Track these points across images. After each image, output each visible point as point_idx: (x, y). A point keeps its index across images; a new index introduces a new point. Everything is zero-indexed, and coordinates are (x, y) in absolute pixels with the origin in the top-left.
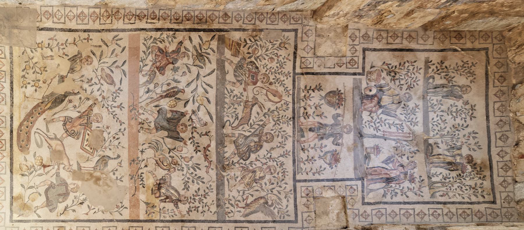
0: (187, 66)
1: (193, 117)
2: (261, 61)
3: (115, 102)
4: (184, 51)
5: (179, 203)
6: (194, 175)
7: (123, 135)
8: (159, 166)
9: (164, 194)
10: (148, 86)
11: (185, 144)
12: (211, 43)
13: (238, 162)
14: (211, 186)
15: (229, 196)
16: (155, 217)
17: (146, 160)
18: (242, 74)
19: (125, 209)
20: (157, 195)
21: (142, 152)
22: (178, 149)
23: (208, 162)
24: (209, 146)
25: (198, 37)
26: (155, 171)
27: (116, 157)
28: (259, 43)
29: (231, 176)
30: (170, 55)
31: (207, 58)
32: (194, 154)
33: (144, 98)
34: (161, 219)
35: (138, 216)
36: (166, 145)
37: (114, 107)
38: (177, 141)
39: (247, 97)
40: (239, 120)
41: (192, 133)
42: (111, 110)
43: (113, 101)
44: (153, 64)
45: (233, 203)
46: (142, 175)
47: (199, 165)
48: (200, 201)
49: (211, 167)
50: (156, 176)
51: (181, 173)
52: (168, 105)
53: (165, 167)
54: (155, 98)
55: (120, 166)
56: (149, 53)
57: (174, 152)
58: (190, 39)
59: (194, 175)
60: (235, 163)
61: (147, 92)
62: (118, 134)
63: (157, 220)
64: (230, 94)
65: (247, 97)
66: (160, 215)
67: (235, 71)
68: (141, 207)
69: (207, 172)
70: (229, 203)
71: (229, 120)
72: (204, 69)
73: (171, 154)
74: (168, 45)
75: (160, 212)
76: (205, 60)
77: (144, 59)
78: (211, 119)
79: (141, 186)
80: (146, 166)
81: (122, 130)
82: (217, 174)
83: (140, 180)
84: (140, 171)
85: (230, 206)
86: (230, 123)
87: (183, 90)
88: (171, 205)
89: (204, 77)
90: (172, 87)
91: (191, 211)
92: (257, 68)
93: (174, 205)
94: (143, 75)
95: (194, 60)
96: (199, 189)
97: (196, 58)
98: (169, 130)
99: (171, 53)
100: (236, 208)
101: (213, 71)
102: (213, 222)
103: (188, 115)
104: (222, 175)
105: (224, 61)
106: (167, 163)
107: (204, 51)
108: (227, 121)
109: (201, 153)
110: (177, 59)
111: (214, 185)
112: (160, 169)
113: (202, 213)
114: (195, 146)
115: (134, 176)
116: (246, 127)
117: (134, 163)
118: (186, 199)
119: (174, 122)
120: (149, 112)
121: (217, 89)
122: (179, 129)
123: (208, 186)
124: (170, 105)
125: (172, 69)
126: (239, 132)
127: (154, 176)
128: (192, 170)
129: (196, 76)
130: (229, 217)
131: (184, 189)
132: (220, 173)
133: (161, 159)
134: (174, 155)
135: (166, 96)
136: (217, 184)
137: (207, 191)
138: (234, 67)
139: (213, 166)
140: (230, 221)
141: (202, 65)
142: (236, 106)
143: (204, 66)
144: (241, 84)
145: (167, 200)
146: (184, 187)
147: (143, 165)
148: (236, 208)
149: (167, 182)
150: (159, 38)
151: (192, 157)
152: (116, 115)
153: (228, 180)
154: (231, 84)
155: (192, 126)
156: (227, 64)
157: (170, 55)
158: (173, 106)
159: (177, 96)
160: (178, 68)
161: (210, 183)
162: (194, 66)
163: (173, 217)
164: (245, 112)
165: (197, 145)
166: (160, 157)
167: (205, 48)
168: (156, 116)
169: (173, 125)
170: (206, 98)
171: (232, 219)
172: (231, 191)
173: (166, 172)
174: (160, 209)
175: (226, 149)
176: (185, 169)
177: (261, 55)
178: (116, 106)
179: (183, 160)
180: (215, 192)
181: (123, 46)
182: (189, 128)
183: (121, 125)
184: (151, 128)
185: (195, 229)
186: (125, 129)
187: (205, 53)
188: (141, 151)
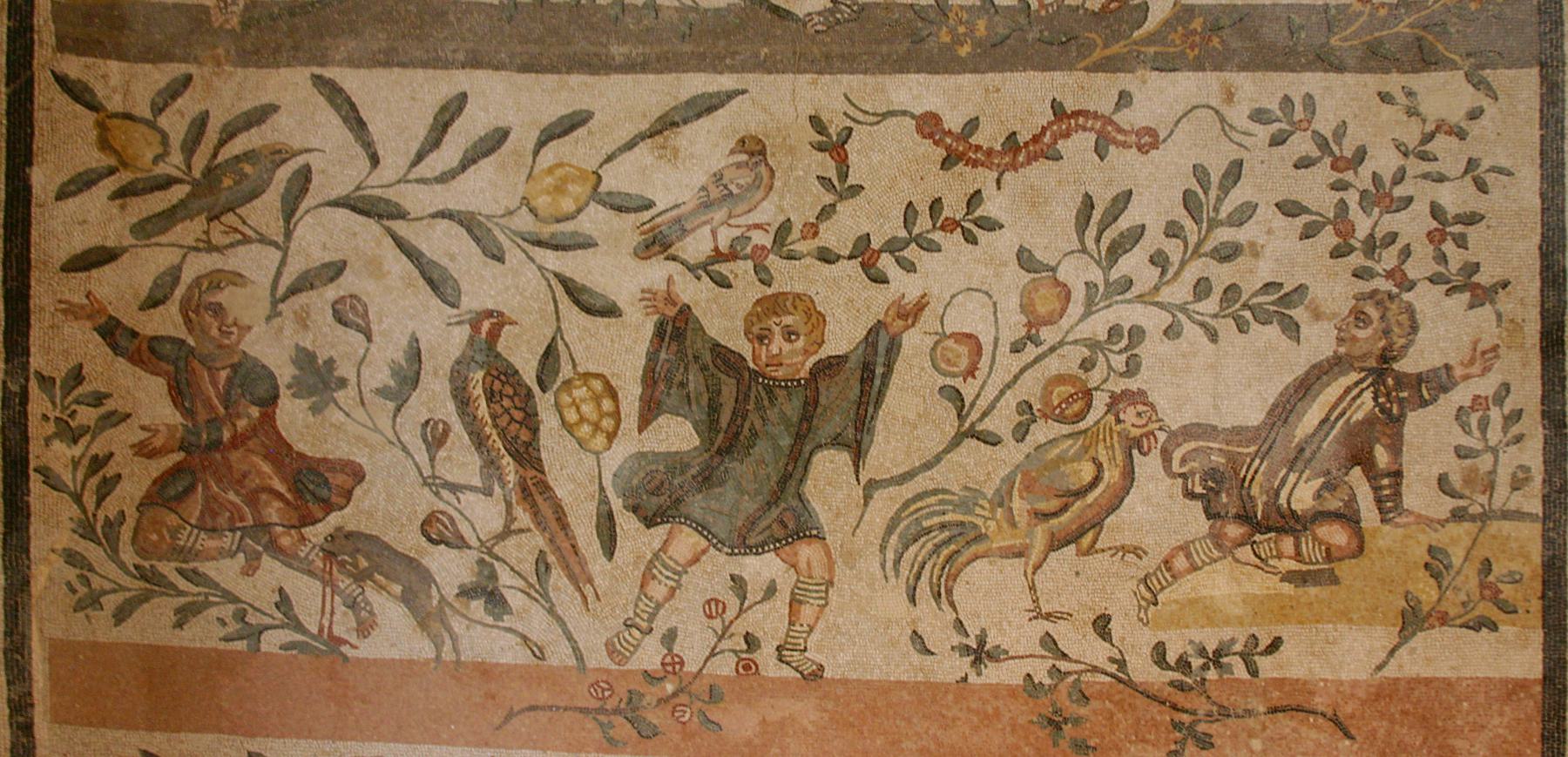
5: (1405, 366)
16: (1527, 557)
22: (964, 363)
34: (1536, 507)
36: (928, 466)
38: (895, 379)
41: (826, 257)
51: (1153, 349)
53: (1111, 475)
57: (982, 403)
63: (1547, 542)
66: (1506, 515)
73: (1001, 422)
88: (1416, 423)
98: (799, 438)
106: (1077, 458)
112: (1122, 512)
119: (742, 398)
133: (1043, 506)
134: (1011, 400)
145: (1382, 457)
149: (1233, 459)
155: (772, 261)
166: (1022, 519)
173: (1148, 466)
182: (788, 277)
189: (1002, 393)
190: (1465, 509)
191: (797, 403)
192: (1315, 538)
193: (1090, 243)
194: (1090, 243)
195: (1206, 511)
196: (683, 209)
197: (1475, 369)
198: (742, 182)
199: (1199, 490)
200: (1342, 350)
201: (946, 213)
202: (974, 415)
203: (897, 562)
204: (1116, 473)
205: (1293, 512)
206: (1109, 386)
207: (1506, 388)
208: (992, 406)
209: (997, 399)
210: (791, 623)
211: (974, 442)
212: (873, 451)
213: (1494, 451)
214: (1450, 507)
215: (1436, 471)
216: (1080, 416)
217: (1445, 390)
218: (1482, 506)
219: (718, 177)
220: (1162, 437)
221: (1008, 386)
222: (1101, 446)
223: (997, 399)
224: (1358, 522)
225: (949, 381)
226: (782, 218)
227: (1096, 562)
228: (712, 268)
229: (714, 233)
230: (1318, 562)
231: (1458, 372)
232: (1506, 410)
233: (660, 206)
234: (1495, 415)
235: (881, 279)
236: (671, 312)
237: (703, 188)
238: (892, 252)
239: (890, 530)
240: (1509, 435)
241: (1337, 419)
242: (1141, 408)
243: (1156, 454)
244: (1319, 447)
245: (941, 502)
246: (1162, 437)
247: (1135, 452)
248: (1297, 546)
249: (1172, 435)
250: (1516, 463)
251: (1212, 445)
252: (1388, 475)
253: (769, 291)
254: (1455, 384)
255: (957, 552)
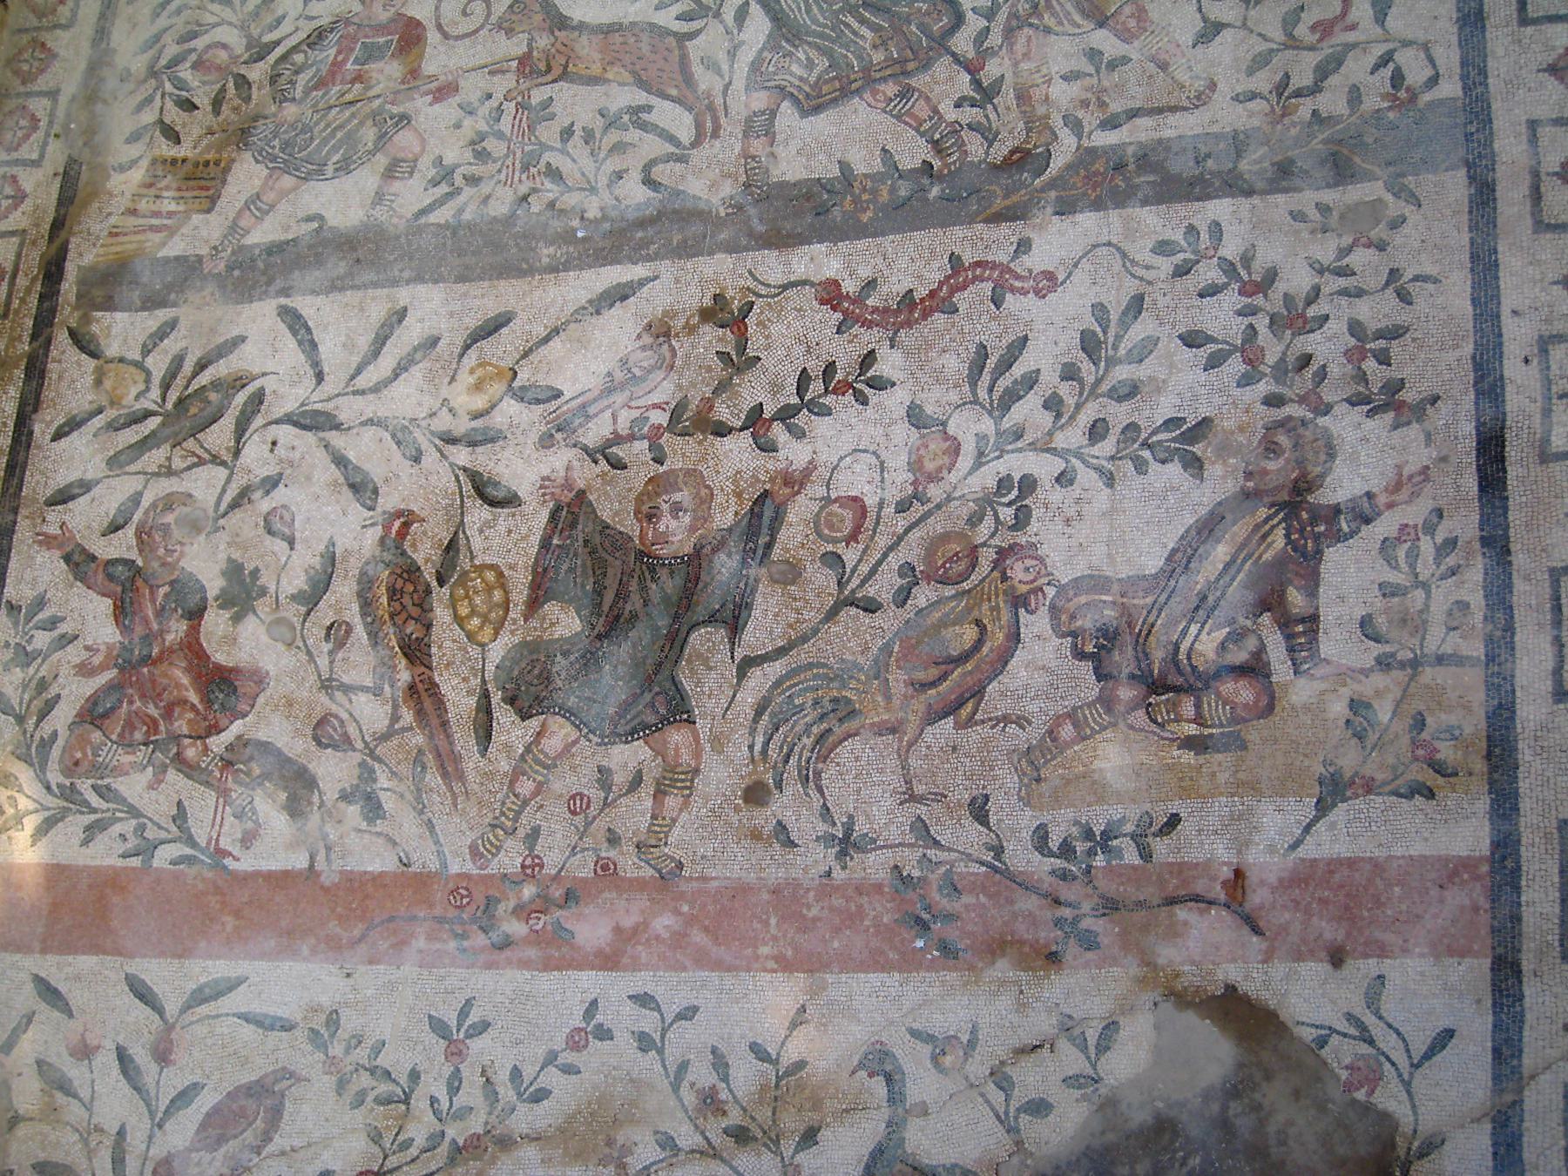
0: (235, 505)
1: (596, 432)
2: (279, 21)
3: (415, 1076)
4: (130, 532)
6: (1066, 391)
7: (688, 1014)
8: (978, 693)
9: (1237, 636)
10: (331, 795)
11: (795, 481)
12: (112, 349)
13: (972, 69)
14: (1164, 248)
15: (1253, 96)
16: (1467, 708)
17: (922, 810)
18: (340, 127)
19: (1389, 1007)
20: (1244, 692)
21: (847, 844)
23: (964, 288)
24: (831, 295)
25: (64, 442)
26: (1022, 721)
27: (879, 1087)
28: (172, 50)
29: (1085, 104)
30: (139, 630)
31: (201, 366)
32: (895, 401)
33: (408, 826)
34: (1477, 649)
35: (1455, 871)
36: (804, 639)
37: (454, 1089)
39: (496, 70)
40: (654, 101)
41: (722, 430)
42: (476, 1125)
43: (406, 1101)
44: (180, 761)
45: (1310, 60)
46: (1054, 843)
47: (982, 352)
48: (1294, 320)
49: (1002, 257)
50: (1071, 715)
52: (488, 631)
53: (998, 637)
54: (418, 739)
55: (972, 1044)
56: (103, 792)
57: (864, 569)
58: (63, 497)
59: (1066, 391)
60: (977, 83)
61: (373, 809)
62: (683, 1067)
63: (1491, 687)
64: (458, 180)
65: (496, 70)
66: (1440, 660)
67: (318, 172)
68: (1366, 848)
69: (1048, 282)
70: (1315, 89)
71: (647, 168)
72: (269, 384)
74: (74, 654)
75: (1415, 664)
76: (216, 385)
77: (141, 828)
78: (624, 298)
79: (1161, 848)
80: (979, 808)
81: (648, 1022)
82: (1065, 209)
83: (1099, 861)
84: (1022, 857)
85: (1333, 80)
86: (669, 158)
87: (387, 528)
88: (1336, 560)
89: (320, 377)
90: (355, 607)
91: (1401, 384)
92: (316, 38)
93: (1340, 537)
94: (247, 840)
95: (201, 462)
96: (1192, 340)
97: (190, 444)
99: (125, 629)
100: (1351, 37)
101: (295, 321)
102: (1484, 195)
103: (575, 474)
104: (1069, 167)
105: (242, 248)
107: (155, 393)
108: (649, 182)
109: (883, 351)
110: (172, 583)
111: (1154, 222)
113: (1404, 297)
114: (829, 400)
115: (1067, 912)
116: (709, 41)
117: (950, 917)
118: (1283, 439)
120: (525, 787)
121: (419, 279)
122: (676, 533)
123: (1166, 265)
124: (485, 619)
125: (237, 619)
126: (739, 84)
127: (1067, 731)
128: (1028, 410)
129: (310, 437)
130: (1434, 81)
131: (1194, 465)
132: (1052, 184)
133: (920, 675)
135: (416, 652)
136: (1145, 202)
137: (1209, 273)
138: (287, 181)
139: (995, 243)
140: (1474, 71)
141: (241, 398)
142: (548, 133)
143: (250, 389)
144: (404, 119)
145: (1296, 599)
146: (1174, 469)
147: (971, 836)
148: (1351, 37)
150: (20, 720)
151: (915, 416)
152: (516, 1073)
153: (1111, 123)
154: (397, 186)
156: (261, 234)
157: (139, 630)
158: (498, 595)
159: (429, 574)
160: (234, 571)
161: (1141, 251)
162: (237, 453)
163: (1451, 543)
164: (596, 69)
165: (816, 387)
167: (134, 391)
168: (560, 732)
169: (644, 589)
170: (467, 347)
171: (1449, 57)
172: (1213, 86)
173: (1036, 624)
174: (1384, 663)
175: (864, 162)
176: (1017, 464)
177: (243, 27)
178: (448, 1070)
179: (935, 492)
180: (1220, 209)
181: (27, 997)
183: (604, 1034)
184: (653, 771)
185: (1559, 338)
186: (644, 1000)
187: (166, 387)
188: (843, 854)
189: (885, 555)
190: (1393, 655)
191: (679, 580)
192: (1218, 695)
193: (983, 394)
194: (983, 394)
195: (1096, 671)
196: (589, 396)
197: (1404, 495)
198: (645, 364)
199: (1090, 648)
200: (1250, 484)
201: (839, 376)
202: (855, 582)
203: (766, 744)
204: (1001, 636)
205: (1194, 668)
206: (996, 541)
207: (1440, 513)
208: (873, 571)
209: (879, 563)
210: (654, 817)
211: (853, 611)
212: (750, 627)
213: (1425, 586)
214: (1375, 654)
215: (1360, 612)
216: (964, 577)
217: (1368, 521)
218: (1412, 650)
219: (624, 362)
220: (1051, 592)
221: (891, 549)
222: (985, 606)
223: (879, 563)
224: (1268, 676)
225: (830, 548)
226: (679, 396)
227: (976, 734)
228: (606, 455)
229: (614, 417)
230: (1222, 726)
231: (1382, 500)
232: (1439, 540)
233: (567, 395)
234: (1426, 546)
235: (768, 448)
236: (567, 496)
237: (609, 374)
238: (783, 420)
239: (759, 713)
240: (1443, 567)
241: (1245, 561)
242: (1029, 562)
243: (1044, 611)
244: (1223, 594)
245: (815, 677)
246: (1051, 592)
247: (1022, 611)
248: (1198, 706)
249: (1062, 589)
250: (1452, 598)
251: (1104, 598)
252: (1303, 621)
253: (661, 469)
254: (1379, 515)
255: (829, 731)
